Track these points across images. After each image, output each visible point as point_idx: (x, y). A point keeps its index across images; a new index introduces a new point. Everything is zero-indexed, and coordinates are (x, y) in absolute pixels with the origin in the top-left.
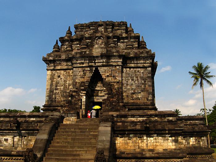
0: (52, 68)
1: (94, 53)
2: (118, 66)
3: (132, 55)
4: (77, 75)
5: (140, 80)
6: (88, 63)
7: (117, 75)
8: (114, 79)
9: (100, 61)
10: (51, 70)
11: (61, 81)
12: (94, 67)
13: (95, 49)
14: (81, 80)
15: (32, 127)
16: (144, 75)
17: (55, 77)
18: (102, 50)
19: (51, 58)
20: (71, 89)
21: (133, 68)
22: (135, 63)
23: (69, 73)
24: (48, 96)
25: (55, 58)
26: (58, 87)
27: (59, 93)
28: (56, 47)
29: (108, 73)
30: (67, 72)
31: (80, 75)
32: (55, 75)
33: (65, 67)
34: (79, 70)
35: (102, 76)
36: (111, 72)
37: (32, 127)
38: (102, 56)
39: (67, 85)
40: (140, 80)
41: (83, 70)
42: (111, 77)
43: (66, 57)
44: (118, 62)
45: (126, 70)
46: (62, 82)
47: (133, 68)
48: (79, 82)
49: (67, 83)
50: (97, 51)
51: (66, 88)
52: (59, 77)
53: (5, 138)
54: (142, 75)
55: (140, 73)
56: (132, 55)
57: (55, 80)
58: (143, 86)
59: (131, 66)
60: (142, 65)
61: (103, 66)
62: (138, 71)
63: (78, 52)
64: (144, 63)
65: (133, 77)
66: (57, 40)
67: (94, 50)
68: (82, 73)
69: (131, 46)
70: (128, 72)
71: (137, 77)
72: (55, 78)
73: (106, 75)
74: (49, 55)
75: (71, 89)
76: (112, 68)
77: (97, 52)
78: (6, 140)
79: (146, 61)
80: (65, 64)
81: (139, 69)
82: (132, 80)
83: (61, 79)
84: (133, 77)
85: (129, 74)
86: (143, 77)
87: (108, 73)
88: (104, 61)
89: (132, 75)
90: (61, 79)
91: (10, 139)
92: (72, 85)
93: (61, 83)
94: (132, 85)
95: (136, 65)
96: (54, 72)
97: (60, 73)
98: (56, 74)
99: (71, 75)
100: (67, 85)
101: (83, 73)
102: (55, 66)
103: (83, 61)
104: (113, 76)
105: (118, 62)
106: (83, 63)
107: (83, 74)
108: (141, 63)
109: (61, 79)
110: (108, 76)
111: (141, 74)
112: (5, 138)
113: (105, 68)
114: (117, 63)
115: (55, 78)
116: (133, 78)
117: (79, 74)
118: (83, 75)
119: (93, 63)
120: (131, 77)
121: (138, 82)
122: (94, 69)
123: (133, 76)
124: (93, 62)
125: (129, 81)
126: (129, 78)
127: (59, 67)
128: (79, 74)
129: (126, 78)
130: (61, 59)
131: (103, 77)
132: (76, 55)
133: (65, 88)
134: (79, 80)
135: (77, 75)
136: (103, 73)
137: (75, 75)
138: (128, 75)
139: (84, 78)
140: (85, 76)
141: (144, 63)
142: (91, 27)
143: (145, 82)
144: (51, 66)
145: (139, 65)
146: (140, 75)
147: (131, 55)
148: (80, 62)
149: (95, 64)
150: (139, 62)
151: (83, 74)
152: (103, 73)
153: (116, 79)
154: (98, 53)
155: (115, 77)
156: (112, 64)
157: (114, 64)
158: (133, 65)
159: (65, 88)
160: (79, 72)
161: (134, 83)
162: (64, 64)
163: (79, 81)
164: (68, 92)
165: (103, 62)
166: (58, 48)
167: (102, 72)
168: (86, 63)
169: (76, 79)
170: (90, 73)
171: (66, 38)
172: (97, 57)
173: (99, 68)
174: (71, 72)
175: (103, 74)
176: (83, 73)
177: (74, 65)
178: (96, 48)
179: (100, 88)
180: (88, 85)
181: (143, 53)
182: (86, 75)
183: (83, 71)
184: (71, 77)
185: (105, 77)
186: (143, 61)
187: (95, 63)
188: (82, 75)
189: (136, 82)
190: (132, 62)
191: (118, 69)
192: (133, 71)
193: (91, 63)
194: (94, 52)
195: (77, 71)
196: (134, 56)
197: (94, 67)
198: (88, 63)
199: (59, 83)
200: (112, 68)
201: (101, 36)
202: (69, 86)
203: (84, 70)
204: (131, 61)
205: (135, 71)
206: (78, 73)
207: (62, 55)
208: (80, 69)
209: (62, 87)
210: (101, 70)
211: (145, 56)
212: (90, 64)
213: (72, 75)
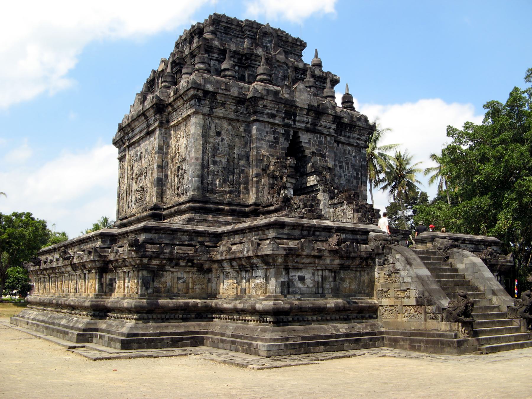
1: (297, 100)
5: (351, 169)
8: (323, 162)
11: (223, 144)
15: (354, 252)
16: (356, 161)
17: (211, 134)
20: (243, 168)
21: (343, 143)
22: (345, 136)
23: (238, 130)
24: (198, 176)
26: (217, 159)
27: (220, 173)
30: (234, 127)
31: (269, 141)
33: (233, 116)
35: (304, 151)
37: (354, 252)
38: (310, 109)
39: (236, 156)
40: (351, 169)
43: (240, 93)
46: (224, 149)
47: (343, 143)
49: (235, 152)
51: (234, 163)
52: (219, 134)
53: (299, 274)
54: (354, 162)
55: (351, 156)
57: (211, 140)
58: (355, 181)
61: (307, 130)
62: (349, 153)
65: (342, 162)
71: (347, 164)
73: (311, 151)
75: (244, 166)
76: (320, 138)
78: (302, 279)
81: (350, 148)
82: (341, 167)
83: (222, 141)
84: (342, 162)
86: (354, 165)
88: (310, 120)
89: (340, 158)
90: (223, 139)
91: (309, 276)
92: (244, 159)
94: (340, 176)
95: (347, 139)
98: (213, 128)
100: (236, 156)
103: (275, 112)
104: (323, 156)
105: (330, 128)
106: (274, 116)
108: (354, 138)
109: (223, 139)
110: (314, 153)
112: (299, 274)
113: (310, 136)
117: (267, 138)
118: (274, 143)
121: (349, 172)
128: (267, 138)
130: (230, 95)
131: (307, 153)
133: (231, 163)
140: (278, 144)
143: (358, 174)
153: (326, 161)
156: (321, 130)
157: (325, 131)
161: (343, 175)
164: (237, 174)
165: (307, 123)
167: (306, 143)
168: (279, 117)
169: (260, 147)
170: (285, 139)
172: (302, 109)
173: (300, 134)
174: (242, 129)
183: (274, 132)
185: (310, 153)
186: (358, 134)
187: (294, 121)
188: (272, 142)
189: (346, 173)
192: (342, 151)
196: (348, 122)
198: (283, 118)
199: (218, 149)
200: (320, 138)
201: (284, 63)
202: (239, 159)
206: (265, 136)
207: (232, 86)
209: (225, 161)
210: (304, 138)
212: (286, 121)
213: (244, 137)
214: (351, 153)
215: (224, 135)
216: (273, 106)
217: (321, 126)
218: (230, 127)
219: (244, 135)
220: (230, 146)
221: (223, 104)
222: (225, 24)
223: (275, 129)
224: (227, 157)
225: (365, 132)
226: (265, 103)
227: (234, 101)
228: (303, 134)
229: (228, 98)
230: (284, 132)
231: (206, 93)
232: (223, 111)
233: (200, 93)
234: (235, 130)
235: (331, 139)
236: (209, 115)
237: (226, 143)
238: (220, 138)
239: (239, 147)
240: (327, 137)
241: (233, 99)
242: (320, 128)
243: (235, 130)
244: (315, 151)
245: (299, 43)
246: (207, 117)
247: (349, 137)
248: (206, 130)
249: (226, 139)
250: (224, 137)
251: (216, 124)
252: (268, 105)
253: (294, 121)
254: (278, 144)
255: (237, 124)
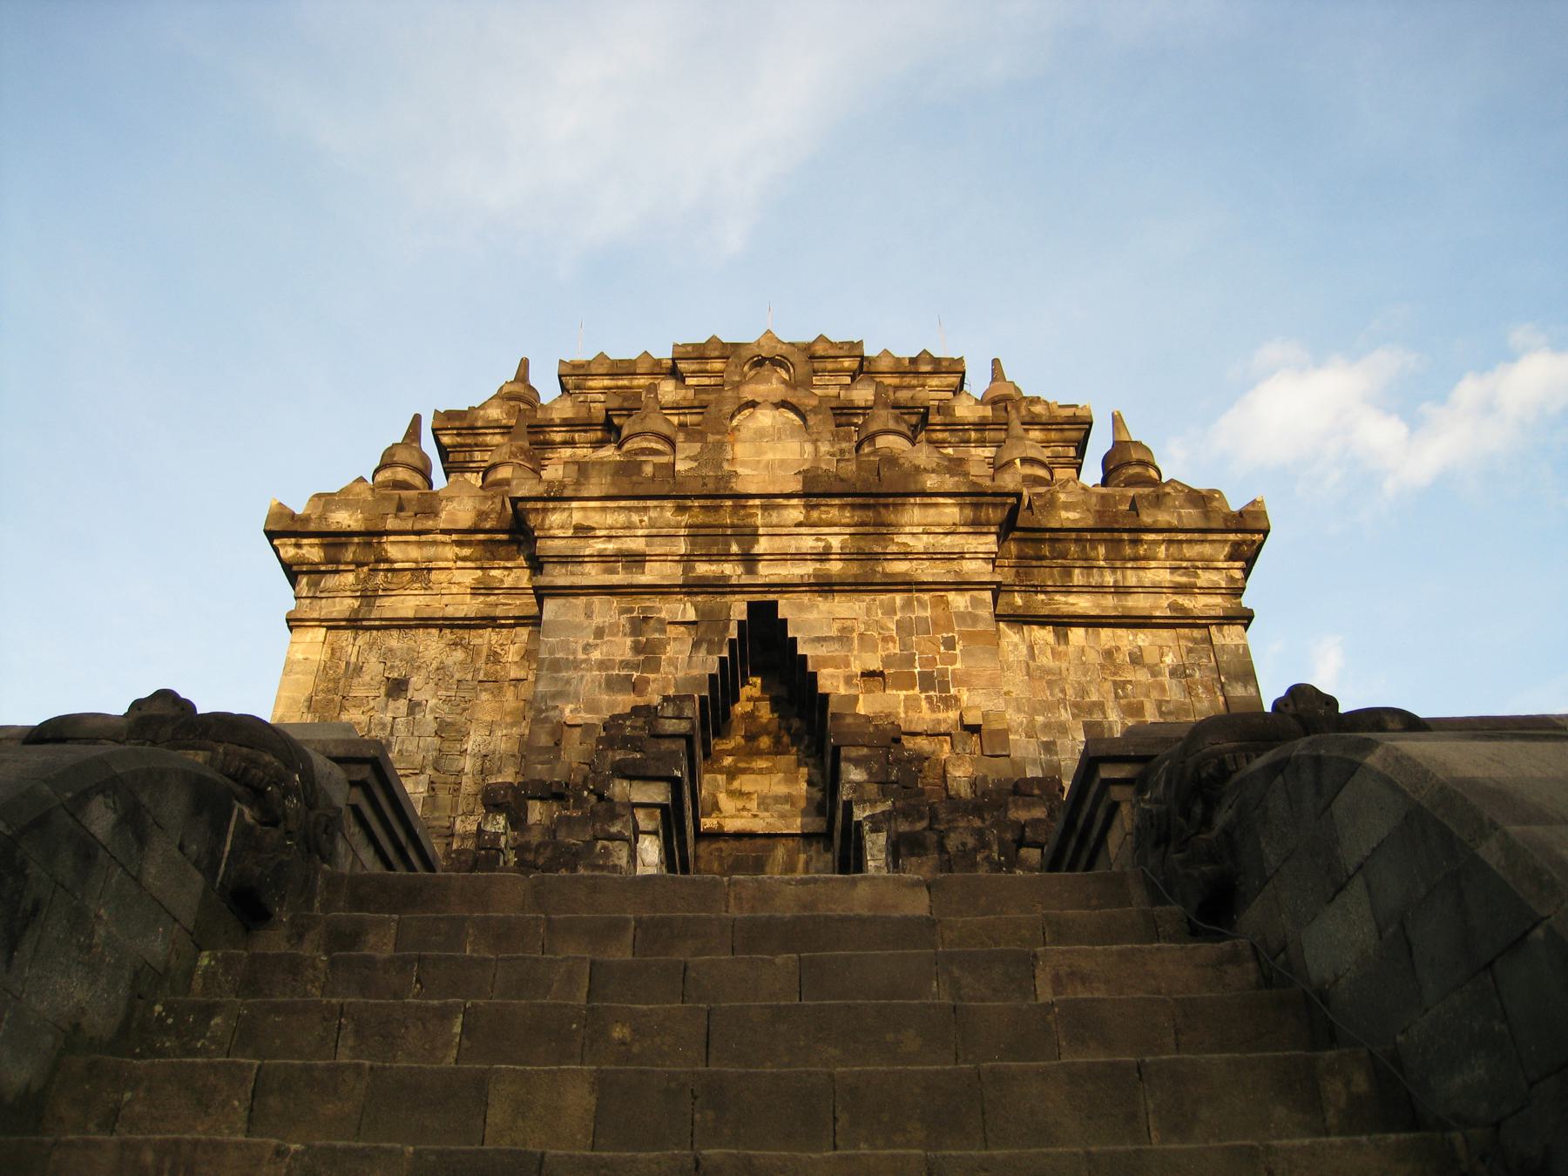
0: (343, 606)
1: (740, 470)
2: (961, 586)
3: (1073, 515)
4: (576, 665)
6: (687, 560)
7: (958, 665)
8: (933, 708)
9: (792, 545)
10: (332, 625)
11: (412, 725)
12: (740, 589)
13: (753, 441)
14: (612, 705)
16: (1189, 690)
17: (358, 692)
18: (816, 450)
19: (344, 519)
22: (1099, 590)
23: (494, 657)
25: (384, 516)
28: (402, 456)
29: (874, 649)
31: (603, 665)
32: (359, 670)
33: (469, 606)
34: (598, 620)
36: (904, 646)
41: (632, 621)
42: (906, 681)
44: (961, 556)
45: (1031, 648)
48: (587, 728)
50: (770, 456)
52: (397, 687)
55: (1155, 673)
56: (1073, 515)
59: (1065, 610)
60: (1164, 601)
61: (824, 587)
63: (601, 463)
64: (1179, 589)
65: (1100, 706)
66: (417, 419)
67: (741, 450)
68: (622, 647)
69: (1042, 473)
70: (1046, 660)
72: (359, 703)
73: (856, 668)
74: (326, 500)
77: (769, 466)
79: (1192, 571)
80: (469, 577)
81: (1143, 638)
85: (1053, 679)
87: (874, 649)
89: (1083, 692)
90: (414, 707)
93: (411, 746)
96: (352, 645)
97: (413, 662)
98: (374, 668)
99: (515, 673)
100: (468, 764)
101: (637, 648)
102: (368, 596)
103: (637, 545)
104: (927, 681)
105: (961, 556)
107: (628, 655)
108: (1156, 589)
109: (414, 707)
111: (1166, 679)
114: (955, 566)
115: (359, 703)
116: (1097, 717)
118: (636, 667)
119: (725, 556)
120: (1075, 705)
122: (738, 609)
123: (1094, 698)
124: (735, 548)
125: (1068, 743)
126: (1065, 715)
127: (406, 604)
128: (596, 655)
129: (1035, 711)
131: (830, 682)
132: (578, 483)
134: (592, 707)
135: (576, 665)
136: (822, 651)
137: (556, 665)
138: (1050, 683)
139: (637, 687)
140: (657, 670)
141: (1179, 589)
142: (694, 374)
144: (333, 594)
145: (1139, 604)
146: (1155, 695)
147: (1064, 514)
148: (611, 547)
149: (751, 570)
150: (1132, 579)
151: (628, 655)
152: (822, 651)
153: (949, 702)
154: (780, 473)
155: (944, 687)
156: (905, 574)
157: (928, 571)
158: (1083, 604)
159: (443, 796)
160: (599, 633)
162: (458, 576)
163: (584, 717)
165: (823, 556)
166: (419, 464)
168: (663, 558)
169: (555, 696)
170: (696, 645)
171: (495, 413)
172: (770, 500)
174: (512, 654)
175: (825, 661)
176: (629, 641)
177: (558, 570)
178: (761, 434)
179: (782, 816)
180: (683, 726)
181: (1168, 501)
182: (664, 667)
183: (639, 625)
184: (509, 694)
185: (848, 680)
186: (1173, 569)
188: (625, 664)
190: (1078, 577)
191: (962, 617)
192: (1093, 657)
193: (710, 558)
194: (744, 464)
195: (578, 627)
197: (740, 589)
200: (908, 605)
203: (646, 619)
204: (1067, 571)
205: (1109, 654)
208: (606, 611)
210: (810, 622)
211: (1187, 524)
214: (1148, 659)
215: (421, 690)
216: (622, 518)
217: (906, 555)
218: (459, 655)
219: (522, 674)
220: (444, 729)
221: (421, 572)
222: (607, 382)
223: (645, 609)
224: (429, 771)
225: (1207, 549)
226: (577, 517)
227: (466, 552)
228: (801, 608)
229: (435, 543)
230: (691, 615)
231: (334, 540)
232: (422, 601)
233: (312, 552)
234: (481, 663)
235: (975, 602)
236: (354, 623)
237: (429, 717)
238: (402, 704)
239: (491, 728)
240: (951, 596)
241: (459, 543)
242: (900, 567)
243: (481, 663)
244: (875, 664)
245: (926, 368)
246: (349, 634)
247: (1121, 590)
248: (336, 681)
249: (432, 702)
250: (417, 697)
251: (387, 655)
252: (594, 519)
253: (750, 560)
254: (657, 670)
255: (486, 638)
